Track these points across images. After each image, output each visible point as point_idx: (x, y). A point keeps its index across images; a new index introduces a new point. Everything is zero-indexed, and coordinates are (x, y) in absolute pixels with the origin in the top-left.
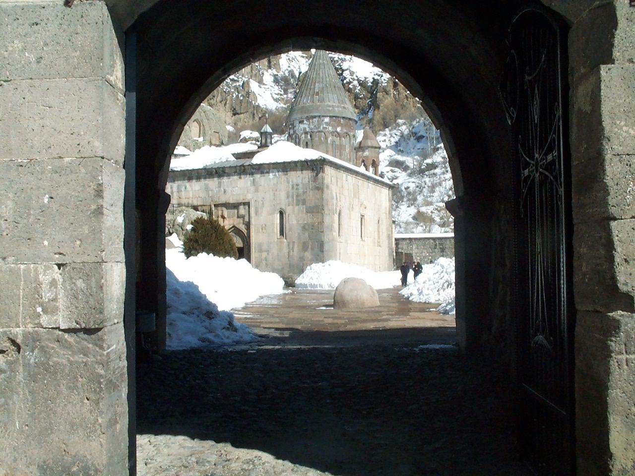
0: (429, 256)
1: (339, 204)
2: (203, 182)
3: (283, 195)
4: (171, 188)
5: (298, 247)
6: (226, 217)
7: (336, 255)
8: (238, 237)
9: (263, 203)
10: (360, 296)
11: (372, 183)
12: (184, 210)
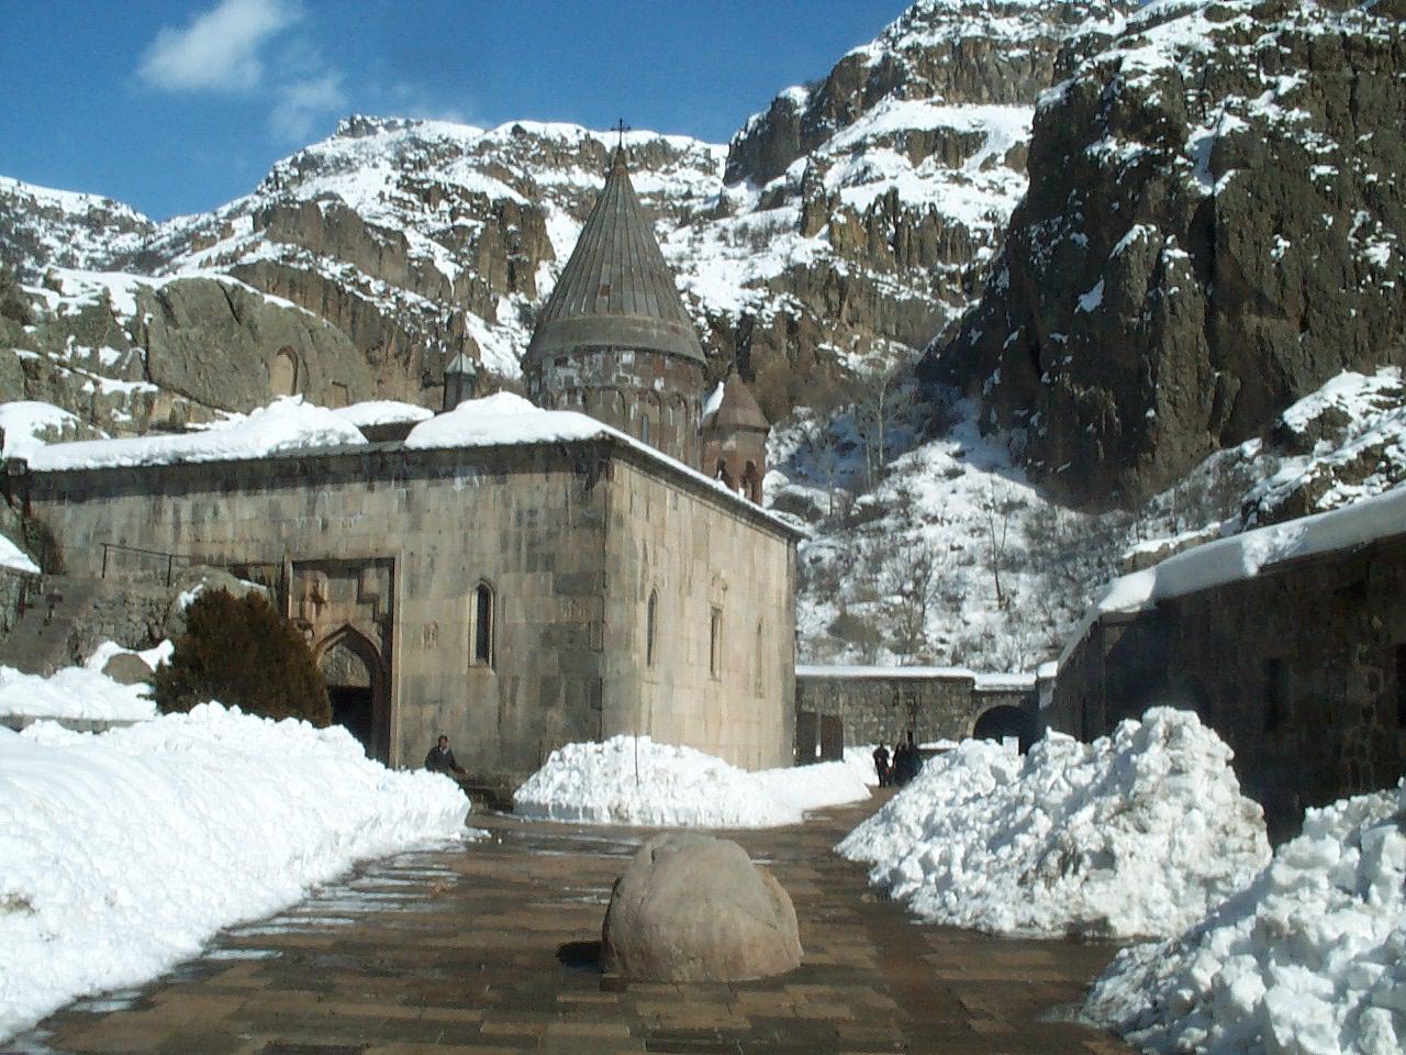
0: (880, 723)
1: (652, 571)
2: (265, 498)
3: (490, 540)
4: (176, 511)
6: (325, 598)
7: (637, 719)
8: (356, 658)
9: (432, 562)
10: (723, 930)
11: (744, 521)
12: (204, 575)
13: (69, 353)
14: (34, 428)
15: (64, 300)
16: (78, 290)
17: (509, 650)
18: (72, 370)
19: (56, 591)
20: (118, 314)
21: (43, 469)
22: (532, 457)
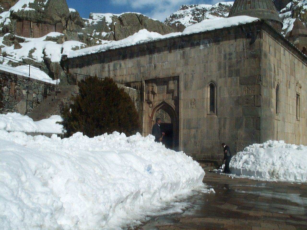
1: (277, 77)
2: (135, 60)
3: (214, 66)
4: (109, 67)
7: (273, 134)
9: (193, 77)
13: (94, 34)
14: (72, 47)
15: (93, 21)
16: (97, 18)
17: (222, 108)
18: (94, 38)
19: (60, 90)
20: (107, 23)
21: (71, 58)
22: (229, 33)
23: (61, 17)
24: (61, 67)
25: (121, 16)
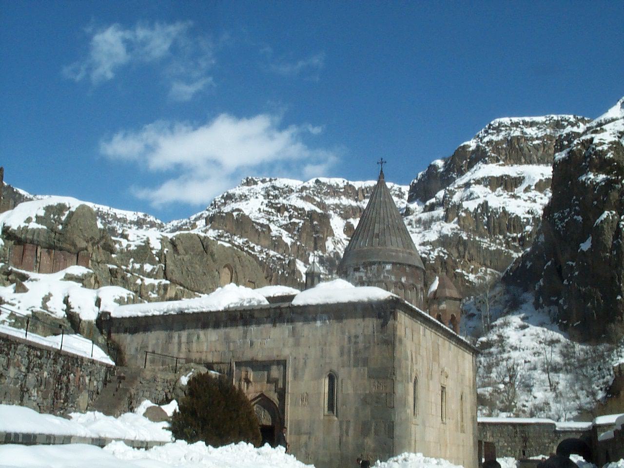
0: (508, 446)
1: (415, 367)
2: (222, 331)
3: (335, 351)
4: (179, 337)
5: (355, 430)
11: (454, 343)
12: (192, 368)
13: (130, 266)
14: (114, 298)
15: (130, 243)
16: (136, 238)
18: (131, 274)
19: (122, 375)
20: (153, 249)
21: (118, 317)
23: (87, 242)
24: (97, 329)
25: (174, 238)
